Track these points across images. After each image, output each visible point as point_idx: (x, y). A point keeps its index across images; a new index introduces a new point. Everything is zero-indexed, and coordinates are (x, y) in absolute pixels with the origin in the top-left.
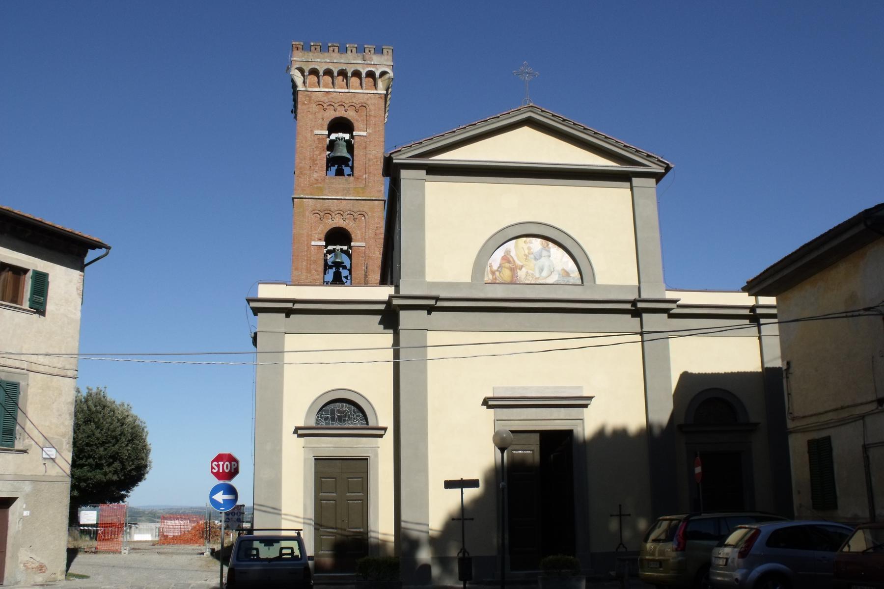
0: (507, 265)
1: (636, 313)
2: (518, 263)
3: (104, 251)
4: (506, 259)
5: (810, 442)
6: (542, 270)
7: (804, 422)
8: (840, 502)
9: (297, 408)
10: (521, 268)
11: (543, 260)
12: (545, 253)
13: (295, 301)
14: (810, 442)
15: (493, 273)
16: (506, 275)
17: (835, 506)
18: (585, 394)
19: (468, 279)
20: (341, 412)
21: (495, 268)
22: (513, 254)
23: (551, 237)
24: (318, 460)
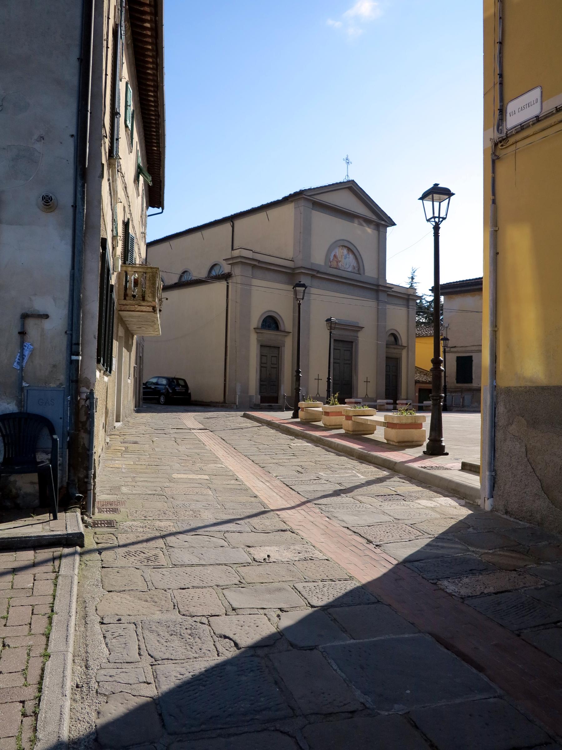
1: (377, 291)
3: (160, 210)
4: (335, 256)
5: (457, 357)
8: (473, 381)
9: (256, 320)
11: (347, 259)
12: (348, 256)
13: (259, 261)
14: (457, 357)
16: (334, 264)
17: (471, 382)
19: (322, 263)
20: (271, 322)
21: (331, 260)
22: (337, 254)
23: (351, 249)
24: (261, 346)
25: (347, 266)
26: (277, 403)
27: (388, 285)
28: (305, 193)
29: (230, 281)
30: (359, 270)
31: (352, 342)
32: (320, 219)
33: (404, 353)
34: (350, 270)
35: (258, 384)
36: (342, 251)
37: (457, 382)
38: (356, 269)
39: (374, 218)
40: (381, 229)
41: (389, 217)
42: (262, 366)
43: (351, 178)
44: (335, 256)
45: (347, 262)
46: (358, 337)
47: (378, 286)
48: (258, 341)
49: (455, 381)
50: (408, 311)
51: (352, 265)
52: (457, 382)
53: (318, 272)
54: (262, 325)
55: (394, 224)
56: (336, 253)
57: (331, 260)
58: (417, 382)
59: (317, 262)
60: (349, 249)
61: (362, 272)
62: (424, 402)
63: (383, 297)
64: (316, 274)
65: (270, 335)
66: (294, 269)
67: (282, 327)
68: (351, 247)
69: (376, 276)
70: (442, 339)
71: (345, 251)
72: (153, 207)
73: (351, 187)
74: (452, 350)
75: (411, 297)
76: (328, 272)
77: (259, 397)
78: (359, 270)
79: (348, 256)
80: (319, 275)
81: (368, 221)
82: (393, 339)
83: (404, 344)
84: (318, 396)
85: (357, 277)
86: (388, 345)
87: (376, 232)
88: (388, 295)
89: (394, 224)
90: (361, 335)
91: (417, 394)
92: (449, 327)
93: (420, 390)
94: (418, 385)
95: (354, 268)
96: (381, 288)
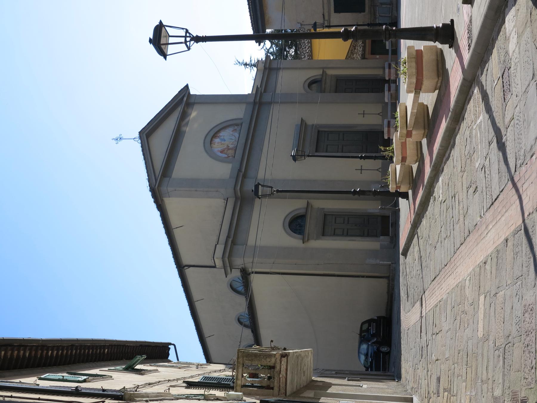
0: (225, 151)
2: (226, 147)
3: (172, 347)
4: (222, 152)
5: (336, 11)
6: (231, 139)
7: (326, 7)
9: (293, 242)
10: (228, 146)
11: (225, 138)
13: (228, 237)
14: (336, 11)
15: (229, 157)
16: (231, 152)
18: (300, 123)
19: (230, 166)
20: (296, 224)
21: (226, 156)
22: (220, 149)
24: (323, 235)
25: (233, 138)
26: (389, 216)
27: (254, 92)
28: (153, 186)
29: (250, 270)
30: (237, 125)
31: (319, 131)
32: (182, 168)
33: (330, 72)
34: (237, 135)
35: (368, 239)
36: (216, 144)
37: (364, 11)
38: (236, 127)
39: (179, 110)
40: (192, 101)
41: (179, 92)
42: (346, 234)
43: (137, 135)
44: (222, 152)
45: (229, 137)
46: (313, 125)
47: (255, 103)
48: (317, 238)
49: (362, 13)
50: (284, 68)
51: (231, 133)
52: (364, 11)
53: (240, 170)
54: (300, 233)
55: (187, 86)
56: (218, 151)
57: (226, 156)
58: (363, 57)
59: (229, 171)
60: (215, 136)
61: (239, 122)
62: (387, 48)
63: (267, 98)
64: (242, 173)
65: (311, 225)
66: (236, 198)
67: (302, 212)
68: (212, 134)
69: (244, 106)
70: (315, 30)
71: (217, 140)
72: (168, 354)
73: (146, 135)
74: (326, 18)
75: (267, 66)
76: (240, 160)
77: (382, 237)
78: (237, 125)
79: (222, 138)
80: (243, 170)
81: (184, 116)
82: (314, 85)
83: (320, 72)
84: (380, 170)
85: (245, 127)
86: (322, 91)
87: (195, 107)
88: (265, 91)
89: (187, 86)
90: (310, 122)
91: (378, 56)
92: (301, 22)
93: (373, 53)
94: (367, 56)
95: (235, 130)
96: (258, 100)
